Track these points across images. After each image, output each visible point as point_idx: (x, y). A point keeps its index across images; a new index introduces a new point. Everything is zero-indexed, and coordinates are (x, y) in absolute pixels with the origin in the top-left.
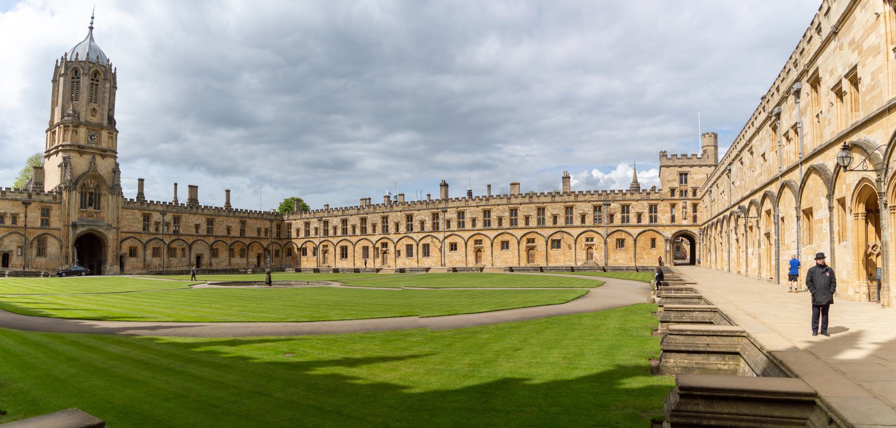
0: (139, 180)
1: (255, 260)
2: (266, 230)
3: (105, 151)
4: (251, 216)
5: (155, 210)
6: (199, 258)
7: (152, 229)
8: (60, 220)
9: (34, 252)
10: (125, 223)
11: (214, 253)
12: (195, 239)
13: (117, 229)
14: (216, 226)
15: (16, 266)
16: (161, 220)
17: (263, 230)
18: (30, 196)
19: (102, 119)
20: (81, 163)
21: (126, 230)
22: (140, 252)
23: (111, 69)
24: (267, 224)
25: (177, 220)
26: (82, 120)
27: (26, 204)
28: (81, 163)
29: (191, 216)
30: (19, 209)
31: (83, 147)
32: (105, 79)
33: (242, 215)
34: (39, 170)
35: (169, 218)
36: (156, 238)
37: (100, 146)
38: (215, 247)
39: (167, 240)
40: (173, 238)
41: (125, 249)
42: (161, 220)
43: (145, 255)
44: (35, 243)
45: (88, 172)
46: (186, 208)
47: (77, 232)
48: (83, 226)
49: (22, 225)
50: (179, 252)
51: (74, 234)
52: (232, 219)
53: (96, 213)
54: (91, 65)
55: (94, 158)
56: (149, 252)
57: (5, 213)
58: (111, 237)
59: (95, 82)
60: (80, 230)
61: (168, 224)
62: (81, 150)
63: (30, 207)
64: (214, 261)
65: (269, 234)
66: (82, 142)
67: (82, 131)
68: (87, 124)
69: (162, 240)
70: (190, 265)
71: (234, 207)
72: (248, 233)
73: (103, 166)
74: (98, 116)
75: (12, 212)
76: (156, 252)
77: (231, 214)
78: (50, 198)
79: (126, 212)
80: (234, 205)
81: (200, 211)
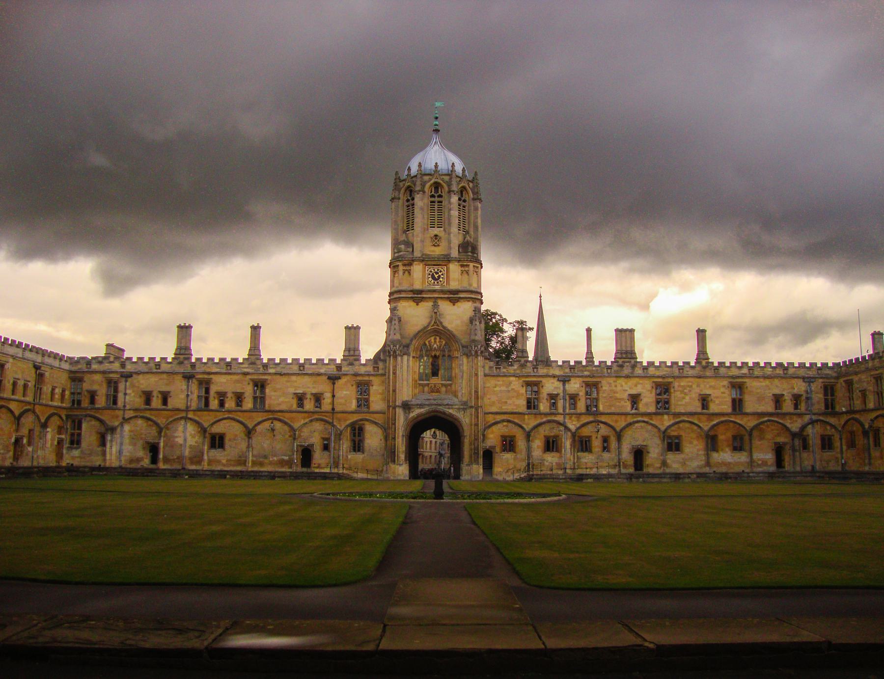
0: (180, 327)
1: (770, 457)
2: (797, 398)
4: (757, 372)
5: (547, 376)
6: (639, 454)
7: (544, 407)
8: (383, 399)
9: (346, 444)
10: (494, 398)
11: (673, 445)
12: (630, 419)
15: (319, 467)
16: (560, 391)
17: (787, 397)
19: (450, 248)
20: (417, 315)
22: (521, 444)
24: (800, 387)
26: (417, 254)
28: (417, 315)
29: (621, 381)
30: (323, 387)
31: (421, 292)
32: (449, 192)
33: (734, 372)
36: (554, 421)
37: (447, 288)
39: (573, 425)
40: (585, 419)
41: (493, 438)
42: (560, 391)
43: (529, 449)
44: (348, 434)
46: (609, 368)
47: (412, 415)
48: (421, 406)
50: (596, 444)
51: (406, 419)
52: (712, 382)
55: (436, 306)
56: (538, 444)
57: (304, 394)
58: (465, 419)
59: (437, 199)
60: (415, 412)
61: (574, 398)
62: (417, 296)
64: (671, 457)
65: (803, 407)
66: (418, 286)
67: (417, 269)
68: (425, 260)
69: (563, 425)
70: (618, 465)
71: (715, 359)
72: (750, 406)
73: (455, 316)
74: (444, 244)
75: (314, 391)
76: (551, 445)
77: (708, 373)
78: (370, 369)
79: (491, 382)
80: (715, 355)
81: (638, 371)
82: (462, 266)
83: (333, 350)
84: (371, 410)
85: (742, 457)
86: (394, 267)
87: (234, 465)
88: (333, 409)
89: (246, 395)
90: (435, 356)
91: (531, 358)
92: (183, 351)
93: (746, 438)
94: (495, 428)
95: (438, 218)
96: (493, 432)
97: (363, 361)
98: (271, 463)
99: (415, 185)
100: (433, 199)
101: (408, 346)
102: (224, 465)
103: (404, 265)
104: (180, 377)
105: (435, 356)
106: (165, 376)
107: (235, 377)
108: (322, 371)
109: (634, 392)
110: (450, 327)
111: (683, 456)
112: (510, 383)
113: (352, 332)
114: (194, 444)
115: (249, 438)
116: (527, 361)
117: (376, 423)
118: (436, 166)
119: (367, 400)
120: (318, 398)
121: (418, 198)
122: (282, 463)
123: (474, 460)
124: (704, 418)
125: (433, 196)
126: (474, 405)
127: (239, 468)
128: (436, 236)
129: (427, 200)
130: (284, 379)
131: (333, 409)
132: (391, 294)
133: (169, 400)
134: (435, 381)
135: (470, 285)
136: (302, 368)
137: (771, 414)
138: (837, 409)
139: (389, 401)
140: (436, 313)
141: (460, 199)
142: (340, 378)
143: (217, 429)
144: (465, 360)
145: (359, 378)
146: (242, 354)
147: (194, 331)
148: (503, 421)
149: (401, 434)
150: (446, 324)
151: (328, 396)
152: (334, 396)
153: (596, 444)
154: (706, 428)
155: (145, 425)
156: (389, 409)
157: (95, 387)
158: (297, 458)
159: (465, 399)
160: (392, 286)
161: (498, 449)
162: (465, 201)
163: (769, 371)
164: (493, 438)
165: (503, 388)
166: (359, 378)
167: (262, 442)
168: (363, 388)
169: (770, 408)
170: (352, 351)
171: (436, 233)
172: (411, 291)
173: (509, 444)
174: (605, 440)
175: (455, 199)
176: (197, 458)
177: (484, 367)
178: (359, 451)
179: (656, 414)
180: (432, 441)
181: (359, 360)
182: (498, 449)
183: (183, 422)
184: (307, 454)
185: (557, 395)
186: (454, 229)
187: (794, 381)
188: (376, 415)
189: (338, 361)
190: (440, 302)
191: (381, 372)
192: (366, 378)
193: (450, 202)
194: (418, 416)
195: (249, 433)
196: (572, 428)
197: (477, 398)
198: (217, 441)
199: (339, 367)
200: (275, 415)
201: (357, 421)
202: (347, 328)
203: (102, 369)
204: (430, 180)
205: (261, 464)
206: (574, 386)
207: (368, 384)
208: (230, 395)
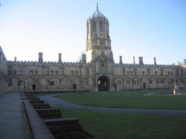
2: (172, 73)
3: (107, 47)
4: (165, 67)
6: (144, 84)
11: (151, 82)
13: (113, 74)
14: (151, 72)
18: (82, 65)
19: (105, 36)
20: (99, 52)
21: (116, 75)
22: (122, 82)
23: (106, 19)
24: (172, 70)
25: (135, 70)
26: (98, 38)
27: (80, 67)
30: (78, 69)
31: (99, 47)
32: (105, 23)
34: (84, 56)
35: (132, 69)
36: (128, 77)
38: (150, 80)
45: (101, 55)
47: (99, 76)
48: (101, 74)
49: (80, 74)
50: (137, 82)
53: (105, 69)
54: (99, 19)
55: (103, 50)
58: (110, 77)
61: (132, 72)
62: (98, 48)
63: (82, 69)
66: (99, 45)
68: (100, 39)
73: (106, 53)
75: (76, 70)
78: (89, 65)
80: (158, 63)
82: (108, 41)
84: (90, 75)
85: (163, 85)
87: (57, 90)
89: (59, 71)
92: (41, 60)
93: (163, 80)
94: (116, 79)
98: (66, 89)
102: (54, 90)
103: (95, 40)
104: (41, 67)
106: (36, 66)
107: (56, 67)
108: (78, 65)
109: (143, 71)
111: (152, 84)
114: (46, 84)
115: (60, 82)
117: (91, 78)
118: (101, 16)
120: (77, 72)
122: (69, 88)
123: (112, 87)
124: (156, 76)
125: (100, 24)
126: (112, 74)
127: (58, 90)
130: (69, 67)
133: (38, 73)
134: (103, 68)
136: (73, 64)
137: (167, 76)
138: (178, 75)
142: (82, 67)
143: (52, 80)
144: (110, 63)
146: (57, 61)
147: (43, 54)
150: (105, 55)
151: (79, 72)
153: (137, 82)
154: (156, 78)
155: (31, 80)
157: (16, 69)
158: (72, 87)
163: (167, 67)
164: (116, 81)
165: (118, 70)
166: (86, 67)
167: (64, 83)
168: (87, 69)
169: (167, 74)
173: (120, 82)
174: (138, 81)
176: (47, 88)
179: (147, 75)
183: (42, 79)
184: (75, 86)
185: (129, 71)
187: (171, 69)
191: (91, 66)
192: (88, 67)
193: (105, 26)
195: (60, 81)
196: (132, 79)
197: (113, 72)
198: (52, 84)
200: (66, 76)
203: (17, 64)
204: (100, 20)
205: (64, 89)
206: (132, 69)
207: (88, 69)
208: (54, 71)
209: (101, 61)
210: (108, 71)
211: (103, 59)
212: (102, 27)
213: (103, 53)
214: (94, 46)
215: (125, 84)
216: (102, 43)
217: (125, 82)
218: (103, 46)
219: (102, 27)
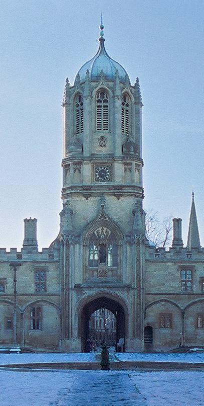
3: (120, 187)
9: (28, 323)
10: (153, 281)
13: (139, 289)
20: (86, 208)
21: (154, 291)
22: (177, 320)
26: (86, 154)
27: (15, 266)
28: (86, 208)
31: (89, 188)
44: (28, 314)
45: (96, 218)
48: (89, 288)
49: (12, 291)
54: (93, 84)
55: (103, 200)
58: (128, 299)
59: (102, 104)
62: (87, 192)
66: (87, 182)
67: (87, 169)
73: (118, 207)
74: (109, 144)
78: (46, 256)
79: (152, 267)
82: (125, 164)
83: (15, 241)
86: (66, 166)
88: (15, 292)
90: (103, 244)
91: (185, 246)
95: (104, 123)
96: (152, 311)
97: (40, 250)
99: (83, 89)
100: (99, 104)
101: (79, 236)
103: (75, 164)
105: (103, 244)
108: (5, 259)
110: (115, 218)
112: (167, 267)
113: (30, 224)
116: (182, 248)
119: (44, 284)
121: (86, 102)
123: (134, 337)
125: (99, 101)
128: (102, 137)
129: (94, 105)
131: (15, 292)
132: (64, 190)
135: (133, 181)
139: (63, 285)
140: (103, 206)
141: (123, 104)
142: (21, 265)
145: (38, 265)
148: (162, 301)
149: (74, 313)
151: (10, 281)
152: (15, 281)
156: (63, 291)
159: (128, 283)
160: (65, 183)
161: (157, 326)
162: (127, 105)
165: (162, 272)
166: (38, 265)
168: (40, 274)
170: (30, 241)
171: (102, 135)
172: (81, 187)
173: (166, 319)
175: (118, 103)
177: (144, 253)
178: (38, 328)
180: (104, 319)
181: (37, 249)
182: (157, 326)
186: (118, 131)
188: (51, 297)
189: (19, 250)
190: (107, 198)
191: (56, 259)
193: (114, 107)
194: (89, 297)
199: (19, 256)
201: (35, 302)
202: (26, 221)
207: (45, 271)
209: (94, 239)
210: (120, 277)
211: (102, 231)
212: (106, 114)
213: (102, 212)
214: (71, 188)
215: (190, 329)
216: (103, 171)
217: (190, 321)
218: (104, 184)
219: (106, 114)
